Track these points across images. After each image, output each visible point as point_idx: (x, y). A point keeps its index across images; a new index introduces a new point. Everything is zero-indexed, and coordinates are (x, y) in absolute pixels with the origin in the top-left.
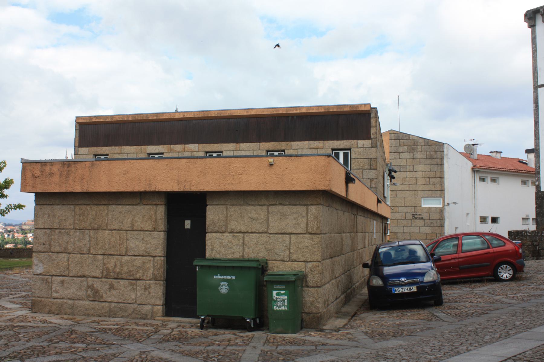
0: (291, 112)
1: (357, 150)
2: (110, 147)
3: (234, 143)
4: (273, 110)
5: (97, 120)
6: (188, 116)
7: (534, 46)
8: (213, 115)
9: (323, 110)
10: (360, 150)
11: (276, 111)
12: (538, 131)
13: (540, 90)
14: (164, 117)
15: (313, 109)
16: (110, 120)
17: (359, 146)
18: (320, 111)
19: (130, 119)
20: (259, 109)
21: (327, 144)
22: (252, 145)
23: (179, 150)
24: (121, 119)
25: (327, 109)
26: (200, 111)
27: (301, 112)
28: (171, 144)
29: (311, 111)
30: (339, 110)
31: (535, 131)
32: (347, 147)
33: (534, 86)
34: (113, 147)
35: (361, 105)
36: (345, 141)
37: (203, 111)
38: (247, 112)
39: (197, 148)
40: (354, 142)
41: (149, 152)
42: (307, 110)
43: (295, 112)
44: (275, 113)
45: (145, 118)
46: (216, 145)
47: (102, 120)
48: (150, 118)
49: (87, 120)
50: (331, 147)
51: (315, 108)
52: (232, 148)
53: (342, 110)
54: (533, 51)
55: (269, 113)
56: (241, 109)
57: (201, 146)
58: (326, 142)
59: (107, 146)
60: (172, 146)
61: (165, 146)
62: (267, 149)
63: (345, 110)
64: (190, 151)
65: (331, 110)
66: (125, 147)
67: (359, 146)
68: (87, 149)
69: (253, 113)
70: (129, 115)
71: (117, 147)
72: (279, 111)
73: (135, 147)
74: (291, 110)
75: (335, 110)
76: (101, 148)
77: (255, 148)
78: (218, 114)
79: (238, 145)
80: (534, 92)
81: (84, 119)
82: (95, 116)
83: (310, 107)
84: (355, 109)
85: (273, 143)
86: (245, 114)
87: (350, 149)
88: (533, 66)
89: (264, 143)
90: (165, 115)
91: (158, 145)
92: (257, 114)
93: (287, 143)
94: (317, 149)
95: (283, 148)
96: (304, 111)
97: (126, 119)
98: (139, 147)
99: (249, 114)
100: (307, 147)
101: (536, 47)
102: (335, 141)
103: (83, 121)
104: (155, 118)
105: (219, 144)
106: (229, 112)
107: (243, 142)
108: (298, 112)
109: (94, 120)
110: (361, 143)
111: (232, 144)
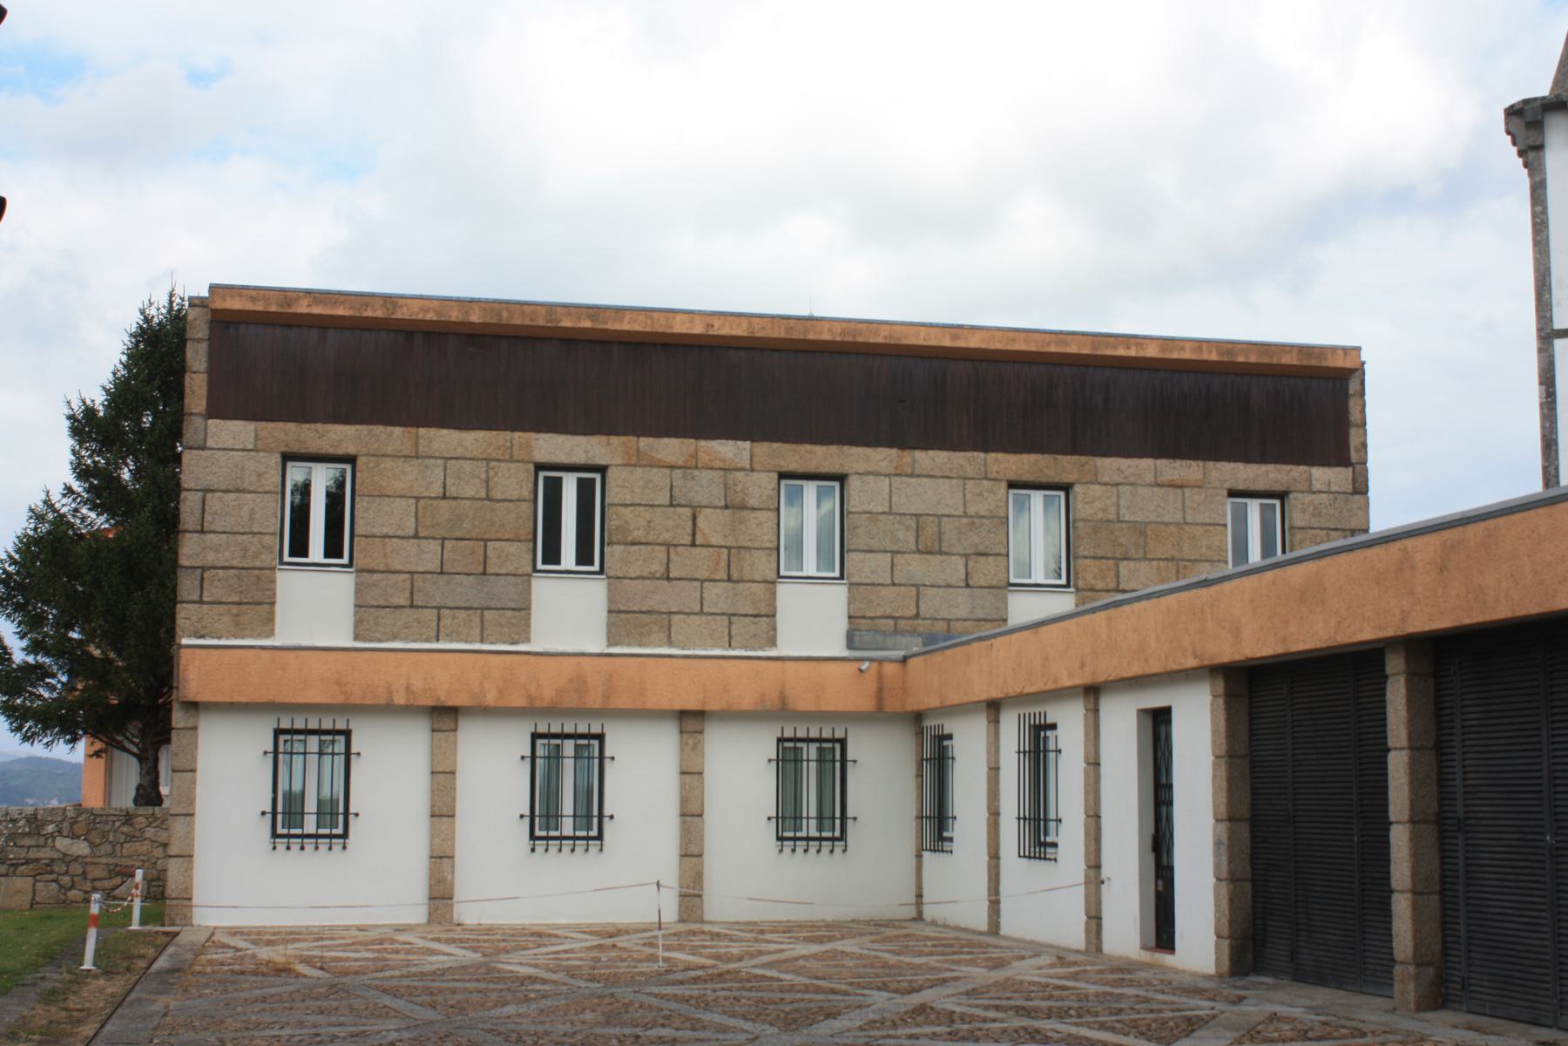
0: (1109, 352)
1: (1308, 498)
2: (364, 429)
3: (890, 446)
4: (1047, 337)
5: (316, 310)
6: (725, 331)
7: (1539, 209)
8: (826, 337)
9: (1214, 357)
10: (1318, 498)
11: (1058, 343)
12: (1557, 469)
13: (1559, 344)
14: (626, 326)
15: (1183, 349)
16: (379, 314)
17: (1317, 486)
18: (1205, 357)
19: (475, 318)
20: (999, 329)
21: (1214, 474)
22: (959, 458)
23: (672, 460)
24: (431, 316)
25: (1229, 352)
26: (773, 317)
27: (1142, 354)
28: (698, 436)
29: (1175, 356)
30: (1266, 360)
31: (1545, 469)
32: (1278, 488)
33: (1539, 330)
34: (378, 429)
35: (1334, 349)
36: (1271, 467)
37: (788, 318)
38: (955, 337)
39: (747, 457)
40: (1298, 471)
41: (541, 457)
42: (1162, 350)
43: (1121, 352)
44: (1053, 349)
45: (541, 322)
46: (820, 450)
47: (341, 311)
48: (567, 323)
49: (266, 300)
50: (1227, 485)
51: (1188, 345)
52: (884, 466)
53: (1275, 361)
54: (1534, 225)
55: (1033, 349)
56: (931, 326)
57: (763, 448)
58: (1210, 464)
59: (347, 420)
60: (644, 442)
61: (615, 440)
62: (1012, 477)
63: (1287, 360)
64: (719, 464)
65: (1241, 359)
66: (433, 431)
67: (1317, 486)
68: (251, 426)
69: (974, 342)
70: (472, 301)
71: (398, 430)
72: (1066, 344)
73: (481, 435)
74: (1107, 346)
75: (1253, 359)
76: (319, 426)
77: (970, 471)
78: (843, 333)
79: (907, 456)
80: (1540, 351)
81: (253, 299)
82: (308, 292)
83: (1173, 340)
84: (1314, 363)
85: (1033, 457)
86: (947, 343)
87: (1282, 496)
88: (1536, 270)
89: (1000, 456)
90: (628, 317)
91: (584, 434)
92: (991, 346)
93: (1083, 459)
94: (1181, 487)
95: (1067, 478)
96: (1151, 352)
97: (455, 315)
98: (500, 438)
99: (961, 344)
100: (1149, 478)
101: (1545, 212)
102: (1241, 466)
103: (249, 306)
104: (587, 324)
105: (833, 449)
106: (885, 331)
107: (925, 448)
108: (1133, 353)
109: (302, 308)
110: (1321, 475)
111: (883, 452)
